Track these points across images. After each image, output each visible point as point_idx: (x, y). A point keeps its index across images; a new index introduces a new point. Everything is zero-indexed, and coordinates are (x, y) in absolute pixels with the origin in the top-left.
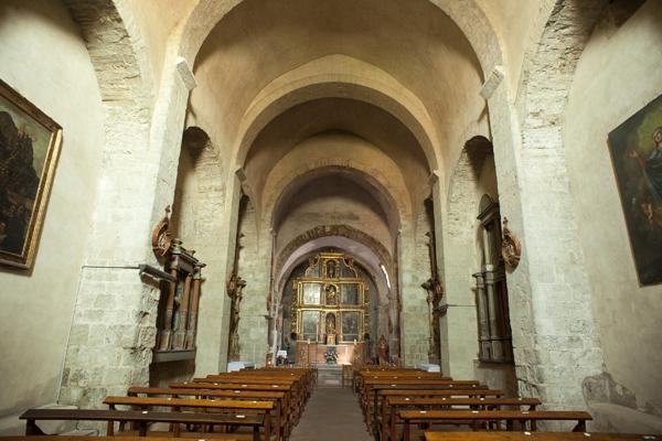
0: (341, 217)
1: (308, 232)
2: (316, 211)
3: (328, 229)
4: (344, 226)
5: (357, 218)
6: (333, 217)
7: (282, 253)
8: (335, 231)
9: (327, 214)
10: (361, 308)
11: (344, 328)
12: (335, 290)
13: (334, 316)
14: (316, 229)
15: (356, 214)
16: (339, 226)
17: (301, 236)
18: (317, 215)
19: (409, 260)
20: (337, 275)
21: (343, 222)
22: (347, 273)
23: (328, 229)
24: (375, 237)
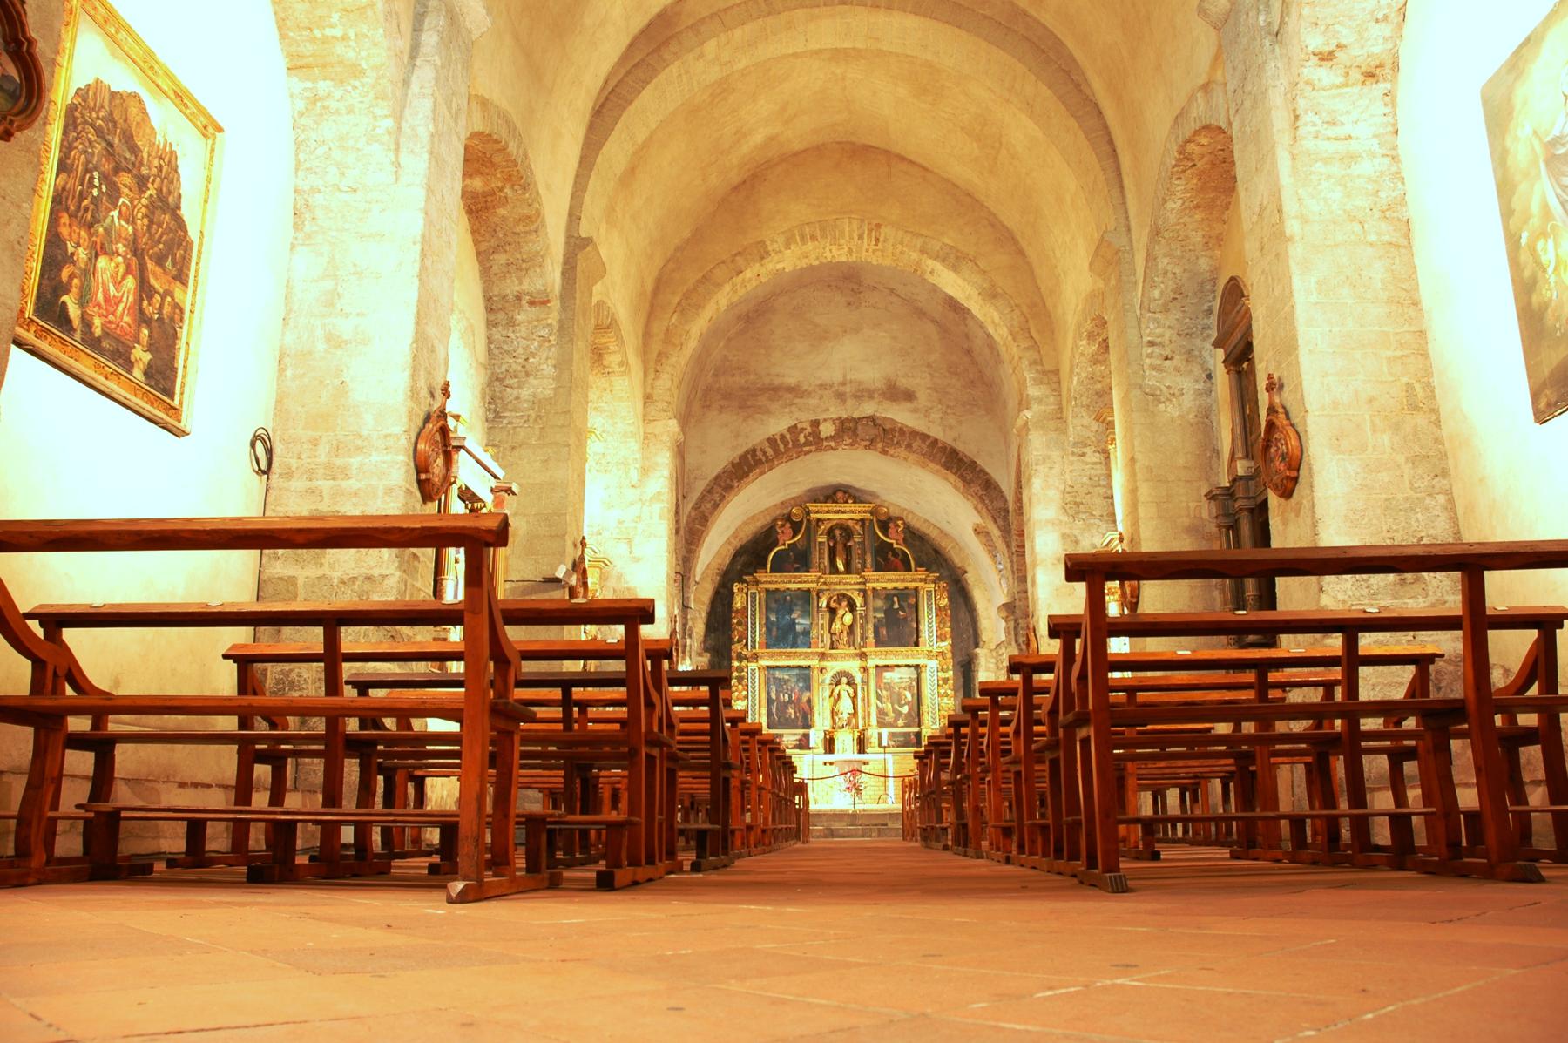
0: (863, 394)
1: (772, 441)
2: (791, 381)
3: (827, 430)
4: (872, 419)
5: (909, 396)
6: (841, 396)
7: (702, 499)
8: (848, 430)
9: (823, 386)
10: (929, 655)
11: (882, 713)
12: (852, 607)
13: (851, 683)
14: (793, 429)
15: (903, 383)
16: (857, 421)
17: (753, 451)
18: (795, 391)
19: (1054, 494)
20: (856, 563)
21: (868, 409)
22: (886, 559)
23: (827, 430)
24: (960, 447)
